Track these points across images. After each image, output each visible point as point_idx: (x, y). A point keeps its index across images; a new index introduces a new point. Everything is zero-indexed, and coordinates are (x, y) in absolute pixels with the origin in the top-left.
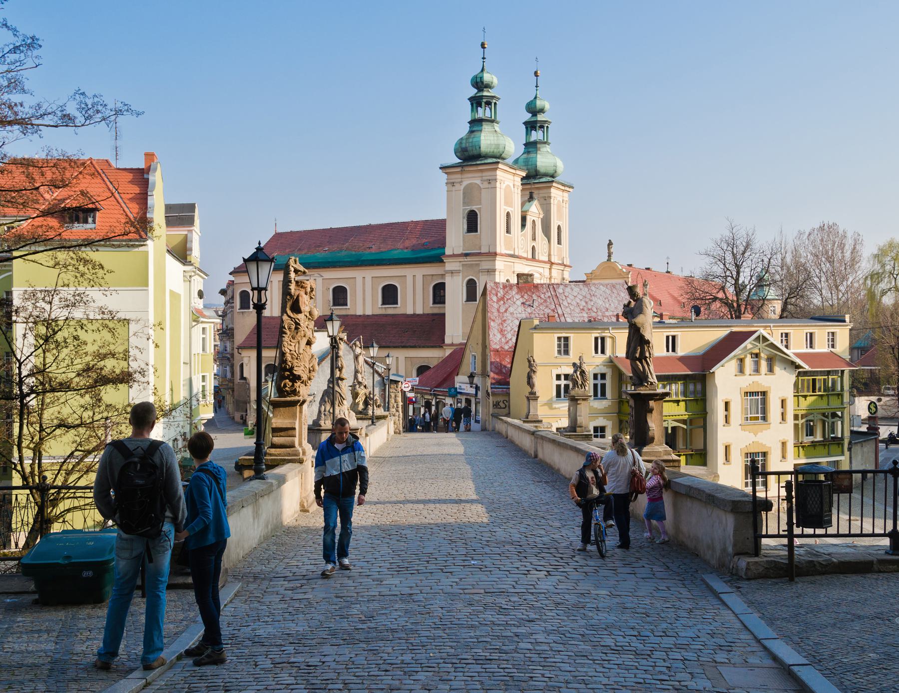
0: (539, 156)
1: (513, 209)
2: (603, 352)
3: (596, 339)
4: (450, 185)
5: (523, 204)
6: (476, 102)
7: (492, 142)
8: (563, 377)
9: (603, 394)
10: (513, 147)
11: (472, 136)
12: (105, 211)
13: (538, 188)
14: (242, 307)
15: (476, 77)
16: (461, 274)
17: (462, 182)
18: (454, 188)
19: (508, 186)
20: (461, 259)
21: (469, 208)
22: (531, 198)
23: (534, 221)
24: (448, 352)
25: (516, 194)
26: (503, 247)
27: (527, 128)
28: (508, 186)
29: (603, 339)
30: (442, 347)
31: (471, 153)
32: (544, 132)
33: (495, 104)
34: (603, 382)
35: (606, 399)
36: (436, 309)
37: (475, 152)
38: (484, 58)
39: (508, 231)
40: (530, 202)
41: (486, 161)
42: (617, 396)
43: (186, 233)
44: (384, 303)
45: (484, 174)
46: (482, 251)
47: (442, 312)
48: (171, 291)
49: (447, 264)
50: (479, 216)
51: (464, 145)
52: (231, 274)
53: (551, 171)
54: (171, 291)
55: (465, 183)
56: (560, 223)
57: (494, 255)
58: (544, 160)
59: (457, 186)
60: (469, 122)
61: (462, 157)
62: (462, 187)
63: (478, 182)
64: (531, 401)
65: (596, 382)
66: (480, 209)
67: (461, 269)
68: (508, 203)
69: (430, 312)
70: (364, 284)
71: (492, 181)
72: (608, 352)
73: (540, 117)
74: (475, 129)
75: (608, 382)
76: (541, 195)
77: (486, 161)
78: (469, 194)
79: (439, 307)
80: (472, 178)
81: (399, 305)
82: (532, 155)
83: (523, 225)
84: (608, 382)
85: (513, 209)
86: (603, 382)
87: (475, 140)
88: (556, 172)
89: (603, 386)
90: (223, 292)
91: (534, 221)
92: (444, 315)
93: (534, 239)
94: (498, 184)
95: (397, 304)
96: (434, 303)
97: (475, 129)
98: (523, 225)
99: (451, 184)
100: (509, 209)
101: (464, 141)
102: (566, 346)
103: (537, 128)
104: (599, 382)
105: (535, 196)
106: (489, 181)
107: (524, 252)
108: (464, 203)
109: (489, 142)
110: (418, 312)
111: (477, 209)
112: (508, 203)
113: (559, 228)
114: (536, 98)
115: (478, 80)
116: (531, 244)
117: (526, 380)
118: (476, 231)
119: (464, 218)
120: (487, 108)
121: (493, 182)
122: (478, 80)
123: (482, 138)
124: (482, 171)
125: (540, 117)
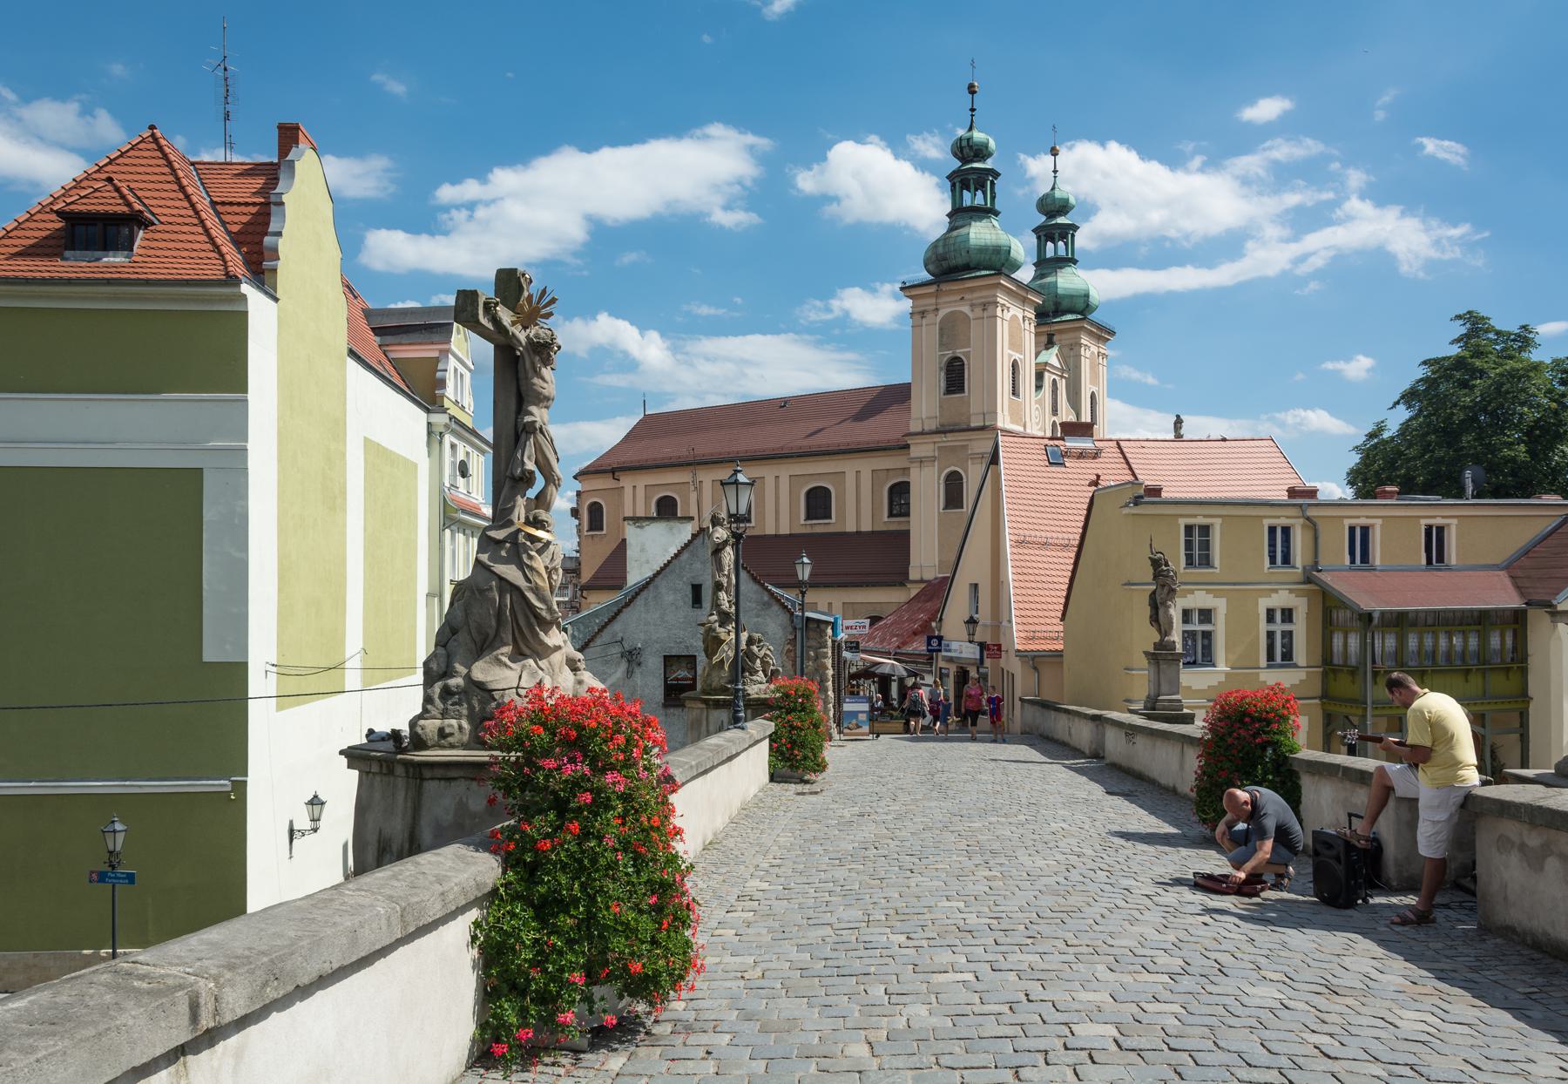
0: (1060, 280)
1: (1022, 357)
2: (1287, 560)
3: (1272, 530)
4: (918, 317)
5: (1037, 355)
6: (960, 181)
7: (989, 242)
8: (1196, 617)
9: (1288, 655)
10: (1022, 248)
11: (955, 233)
12: (160, 227)
13: (1061, 332)
14: (591, 529)
15: (961, 139)
16: (936, 463)
17: (937, 309)
18: (924, 321)
19: (1014, 317)
20: (937, 438)
21: (949, 354)
22: (1050, 344)
23: (1054, 380)
24: (914, 592)
25: (1027, 333)
26: (1008, 419)
27: (1039, 238)
28: (1014, 317)
29: (1286, 531)
30: (902, 584)
31: (953, 263)
32: (1066, 244)
33: (992, 183)
34: (1287, 627)
35: (1295, 666)
36: (895, 525)
37: (960, 261)
38: (973, 110)
39: (1015, 392)
40: (1047, 349)
41: (978, 274)
42: (1318, 659)
43: (436, 354)
44: (808, 517)
45: (976, 295)
46: (973, 425)
47: (903, 528)
48: (370, 446)
49: (912, 448)
50: (966, 367)
51: (940, 250)
52: (575, 477)
53: (1080, 305)
54: (368, 444)
55: (942, 313)
56: (1094, 389)
57: (989, 429)
58: (1067, 286)
59: (930, 317)
60: (949, 215)
61: (937, 271)
62: (938, 321)
63: (966, 309)
64: (1163, 666)
65: (1272, 628)
66: (967, 354)
67: (936, 454)
68: (1016, 345)
69: (885, 529)
70: (777, 488)
71: (989, 305)
72: (1299, 556)
73: (1061, 220)
74: (960, 223)
75: (1299, 628)
76: (1063, 342)
77: (978, 274)
78: (951, 330)
79: (899, 522)
80: (953, 303)
81: (833, 520)
82: (1049, 279)
83: (1039, 387)
84: (1299, 628)
85: (1022, 357)
86: (1287, 627)
87: (959, 240)
88: (1088, 305)
89: (1288, 635)
90: (575, 513)
91: (1054, 380)
92: (908, 532)
93: (1055, 411)
94: (999, 309)
95: (831, 518)
96: (891, 515)
97: (957, 224)
98: (1039, 387)
99: (918, 314)
100: (1017, 356)
101: (941, 243)
102: (1206, 546)
103: (1057, 236)
104: (1279, 627)
105: (1055, 338)
106: (985, 306)
107: (1039, 430)
108: (943, 345)
109: (982, 242)
110: (863, 530)
111: (963, 353)
112: (1016, 345)
113: (1093, 396)
114: (1053, 189)
115: (964, 143)
116: (1050, 419)
117: (1147, 611)
118: (961, 389)
119: (941, 369)
120: (979, 193)
121: (990, 308)
122: (964, 143)
123: (972, 235)
124: (972, 290)
125: (1061, 220)
